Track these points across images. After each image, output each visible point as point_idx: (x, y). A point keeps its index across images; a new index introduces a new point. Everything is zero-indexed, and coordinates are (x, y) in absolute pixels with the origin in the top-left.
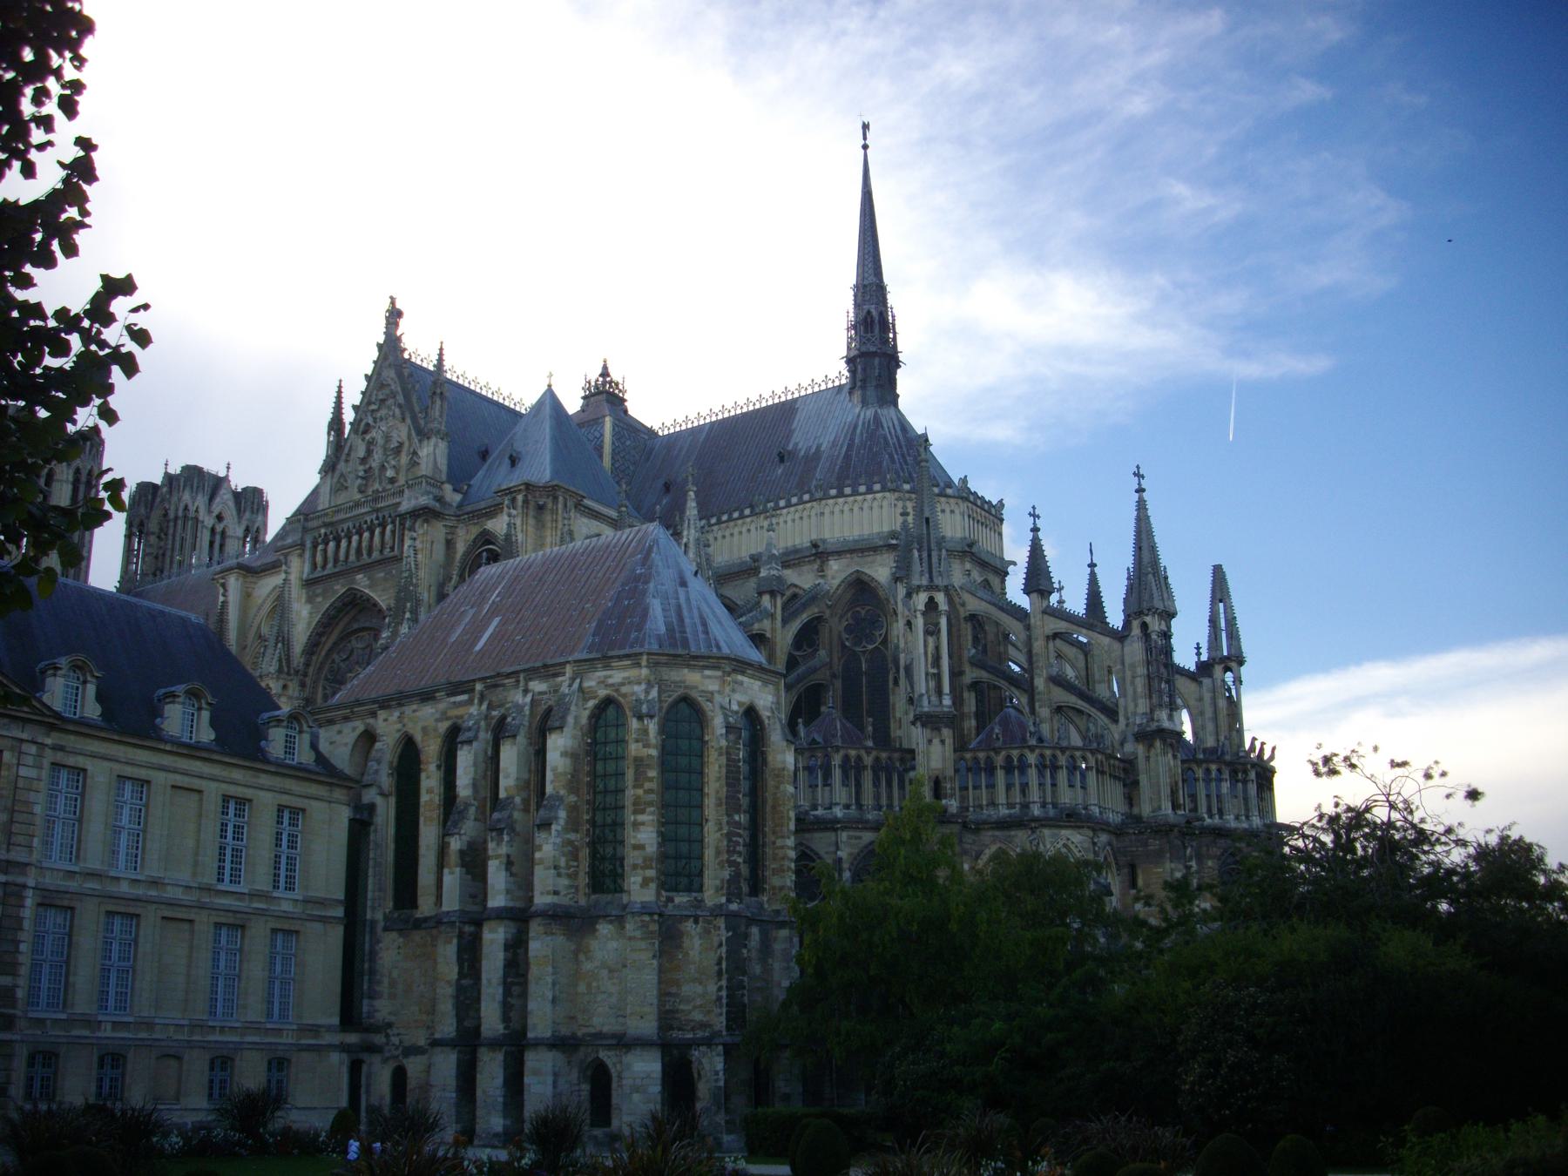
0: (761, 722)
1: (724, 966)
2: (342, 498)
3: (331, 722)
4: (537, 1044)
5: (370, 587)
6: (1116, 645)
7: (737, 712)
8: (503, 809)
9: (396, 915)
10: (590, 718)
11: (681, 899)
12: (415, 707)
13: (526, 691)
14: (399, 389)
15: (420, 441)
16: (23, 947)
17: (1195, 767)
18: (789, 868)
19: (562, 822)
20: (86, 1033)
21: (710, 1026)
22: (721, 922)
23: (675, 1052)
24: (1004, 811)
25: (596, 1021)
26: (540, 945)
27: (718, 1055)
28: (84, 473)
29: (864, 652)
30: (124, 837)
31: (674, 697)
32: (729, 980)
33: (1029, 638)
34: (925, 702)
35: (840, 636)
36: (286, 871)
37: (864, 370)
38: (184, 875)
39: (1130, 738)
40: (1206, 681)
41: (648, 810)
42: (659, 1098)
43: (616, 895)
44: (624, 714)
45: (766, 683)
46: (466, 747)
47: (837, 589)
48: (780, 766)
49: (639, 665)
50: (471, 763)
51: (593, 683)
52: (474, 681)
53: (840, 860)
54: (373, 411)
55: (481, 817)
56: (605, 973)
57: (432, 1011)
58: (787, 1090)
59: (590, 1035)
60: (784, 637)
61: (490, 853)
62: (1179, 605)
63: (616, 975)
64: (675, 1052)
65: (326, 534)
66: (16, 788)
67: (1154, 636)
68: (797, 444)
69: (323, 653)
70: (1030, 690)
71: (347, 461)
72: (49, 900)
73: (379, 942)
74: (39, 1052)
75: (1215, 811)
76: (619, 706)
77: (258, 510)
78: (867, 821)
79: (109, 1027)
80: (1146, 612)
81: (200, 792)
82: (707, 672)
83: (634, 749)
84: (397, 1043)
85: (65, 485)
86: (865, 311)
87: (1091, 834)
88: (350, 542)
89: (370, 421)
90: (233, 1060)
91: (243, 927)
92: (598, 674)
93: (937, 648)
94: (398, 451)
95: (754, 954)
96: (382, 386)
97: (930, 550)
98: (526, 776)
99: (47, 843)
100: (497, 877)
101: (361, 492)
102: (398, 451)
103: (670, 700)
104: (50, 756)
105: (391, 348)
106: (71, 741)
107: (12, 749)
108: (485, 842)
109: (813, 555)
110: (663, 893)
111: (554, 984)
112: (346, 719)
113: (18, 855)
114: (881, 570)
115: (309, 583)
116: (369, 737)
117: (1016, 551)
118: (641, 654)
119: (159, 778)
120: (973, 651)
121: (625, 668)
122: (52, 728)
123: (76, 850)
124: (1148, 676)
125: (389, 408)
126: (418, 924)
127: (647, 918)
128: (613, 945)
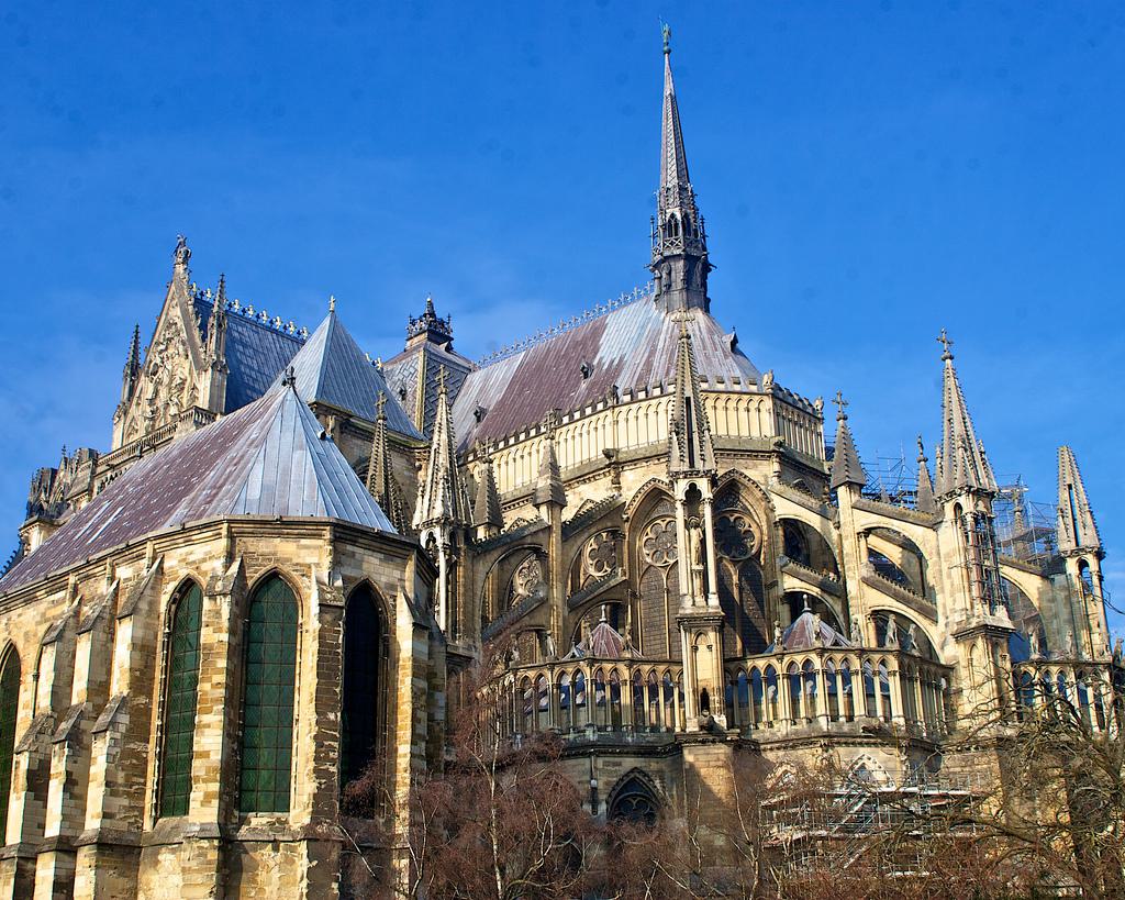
0: (384, 603)
7: (337, 589)
12: (19, 611)
15: (198, 374)
19: (122, 729)
22: (303, 848)
31: (262, 572)
34: (688, 602)
39: (952, 640)
41: (215, 708)
52: (67, 573)
53: (594, 789)
54: (161, 352)
68: (601, 358)
71: (138, 404)
78: (627, 745)
80: (958, 491)
86: (668, 216)
89: (158, 361)
93: (703, 542)
97: (690, 433)
103: (257, 575)
109: (608, 466)
110: (236, 813)
118: (221, 522)
127: (205, 844)
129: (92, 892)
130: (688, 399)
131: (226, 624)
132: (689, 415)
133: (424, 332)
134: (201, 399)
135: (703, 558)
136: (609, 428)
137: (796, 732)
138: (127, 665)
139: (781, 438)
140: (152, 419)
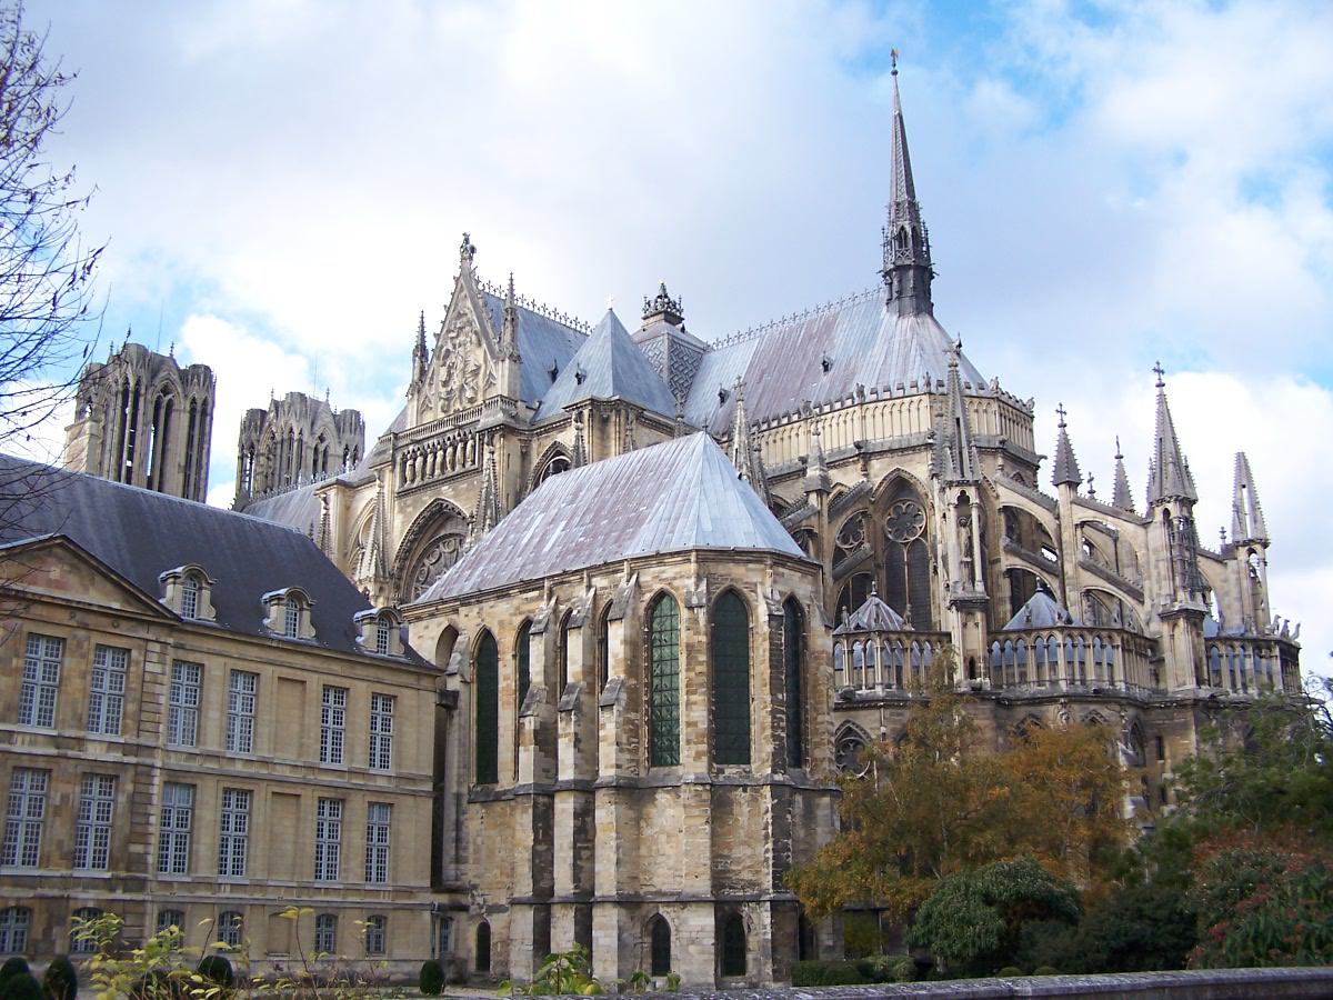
0: (802, 610)
1: (770, 831)
2: (429, 417)
3: (419, 619)
4: (603, 902)
5: (455, 497)
6: (1141, 531)
7: (778, 602)
8: (569, 693)
9: (479, 789)
10: (646, 609)
11: (731, 771)
12: (492, 603)
13: (589, 587)
14: (475, 317)
16: (153, 819)
17: (1218, 643)
18: (830, 742)
19: (623, 703)
20: (208, 894)
21: (759, 885)
22: (767, 791)
23: (726, 908)
24: (1034, 688)
25: (656, 881)
26: (606, 813)
27: (766, 911)
28: (199, 402)
29: (905, 544)
30: (238, 723)
32: (774, 843)
33: (1059, 526)
35: (883, 528)
36: (380, 752)
37: (900, 282)
38: (291, 756)
40: (1231, 563)
42: (712, 949)
43: (674, 768)
44: (677, 605)
45: (805, 574)
46: (537, 638)
47: (879, 487)
48: (820, 649)
49: (689, 560)
50: (543, 652)
51: (649, 578)
52: (543, 579)
54: (452, 338)
55: (552, 698)
56: (663, 838)
57: (512, 873)
58: (831, 943)
59: (651, 893)
60: (831, 534)
61: (560, 732)
62: (1200, 492)
63: (673, 839)
64: (726, 908)
65: (413, 451)
66: (143, 681)
67: (1176, 522)
69: (416, 558)
70: (1059, 574)
71: (431, 384)
72: (175, 779)
73: (464, 813)
74: (168, 911)
75: (1239, 686)
76: (672, 598)
77: (355, 429)
79: (228, 888)
81: (303, 682)
82: (750, 566)
83: (684, 636)
84: (482, 903)
85: (182, 414)
87: (1117, 708)
88: (435, 457)
90: (336, 918)
91: (343, 801)
92: (652, 569)
93: (970, 538)
94: (475, 373)
95: (798, 820)
96: (460, 316)
97: (961, 448)
98: (591, 663)
99: (172, 730)
100: (566, 752)
101: (443, 411)
102: (475, 373)
103: (718, 591)
104: (172, 654)
105: (466, 280)
106: (190, 641)
107: (139, 648)
108: (556, 722)
110: (715, 765)
111: (618, 847)
112: (432, 615)
113: (145, 740)
114: (919, 469)
115: (402, 494)
116: (451, 634)
117: (1044, 441)
118: (690, 551)
119: (268, 673)
120: (1008, 540)
121: (676, 563)
122: (172, 628)
123: (196, 735)
124: (1171, 559)
125: (467, 335)
126: (498, 798)
127: (700, 788)
128: (670, 812)
129: (614, 820)
130: (958, 419)
131: (703, 629)
132: (959, 433)
133: (660, 313)
134: (499, 386)
135: (969, 551)
136: (857, 423)
137: (1041, 692)
138: (621, 656)
139: (1004, 437)
140: (446, 399)
